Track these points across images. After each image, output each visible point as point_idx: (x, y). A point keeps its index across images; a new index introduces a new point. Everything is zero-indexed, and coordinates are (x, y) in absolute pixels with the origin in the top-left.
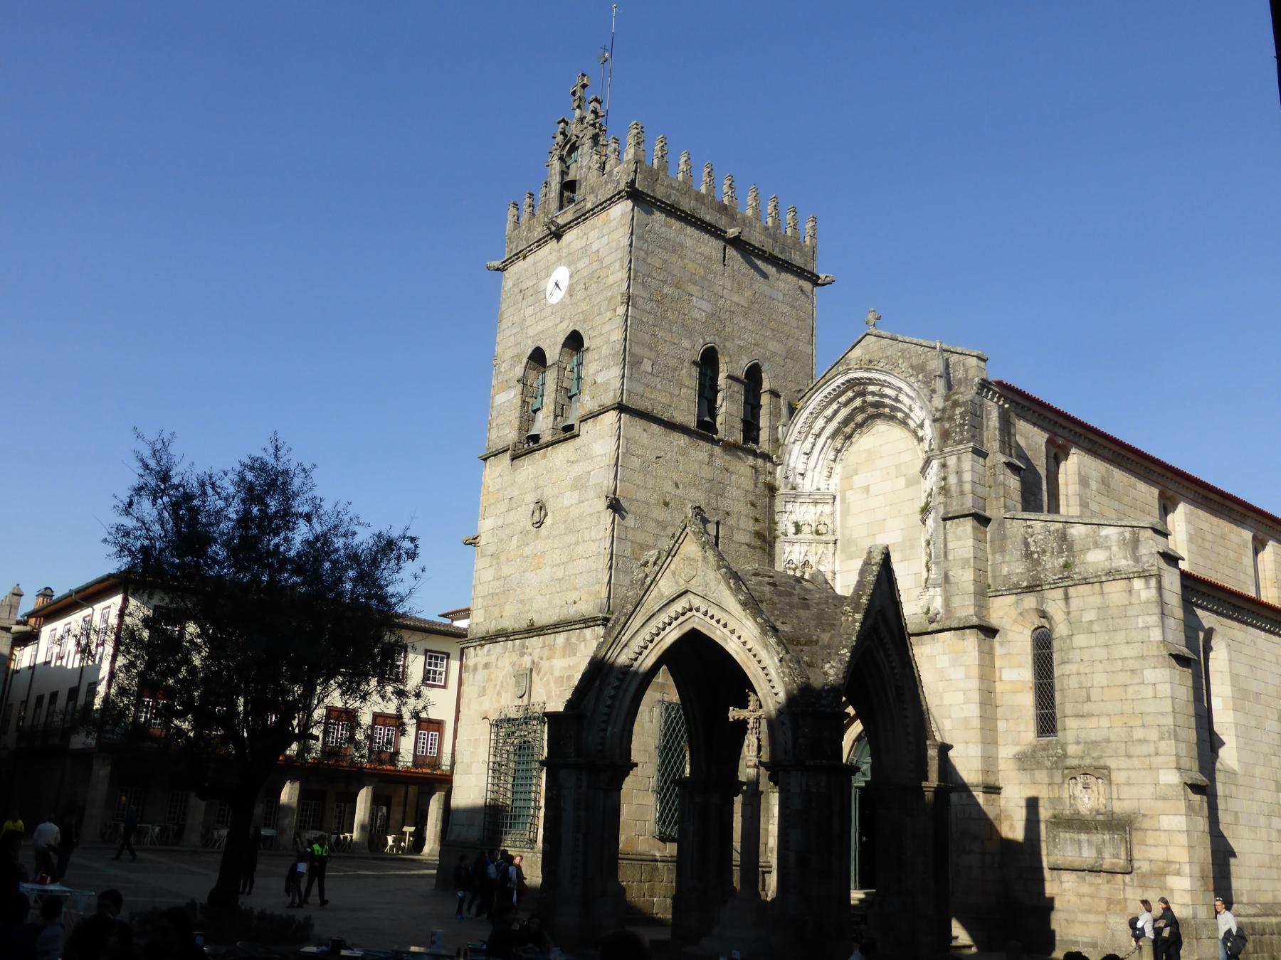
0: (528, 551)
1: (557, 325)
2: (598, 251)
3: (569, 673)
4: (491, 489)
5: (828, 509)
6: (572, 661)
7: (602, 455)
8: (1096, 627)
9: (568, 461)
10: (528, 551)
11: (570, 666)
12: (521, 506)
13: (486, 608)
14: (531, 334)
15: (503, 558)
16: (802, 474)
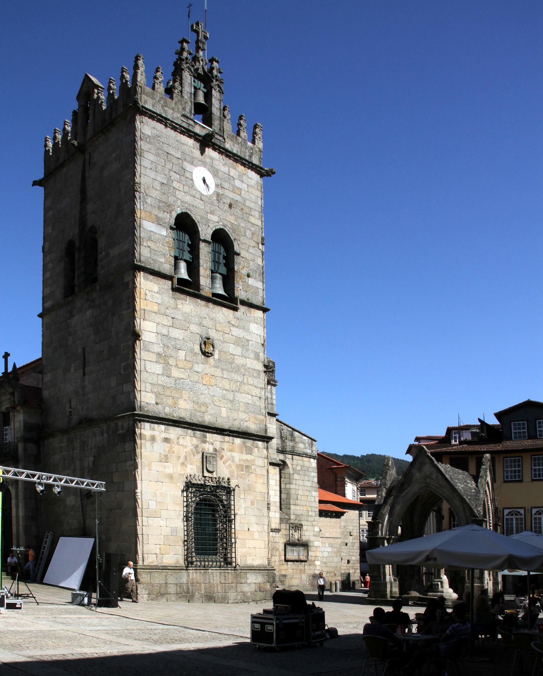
6: (249, 457)
8: (301, 472)
9: (229, 322)
12: (187, 330)
15: (172, 362)
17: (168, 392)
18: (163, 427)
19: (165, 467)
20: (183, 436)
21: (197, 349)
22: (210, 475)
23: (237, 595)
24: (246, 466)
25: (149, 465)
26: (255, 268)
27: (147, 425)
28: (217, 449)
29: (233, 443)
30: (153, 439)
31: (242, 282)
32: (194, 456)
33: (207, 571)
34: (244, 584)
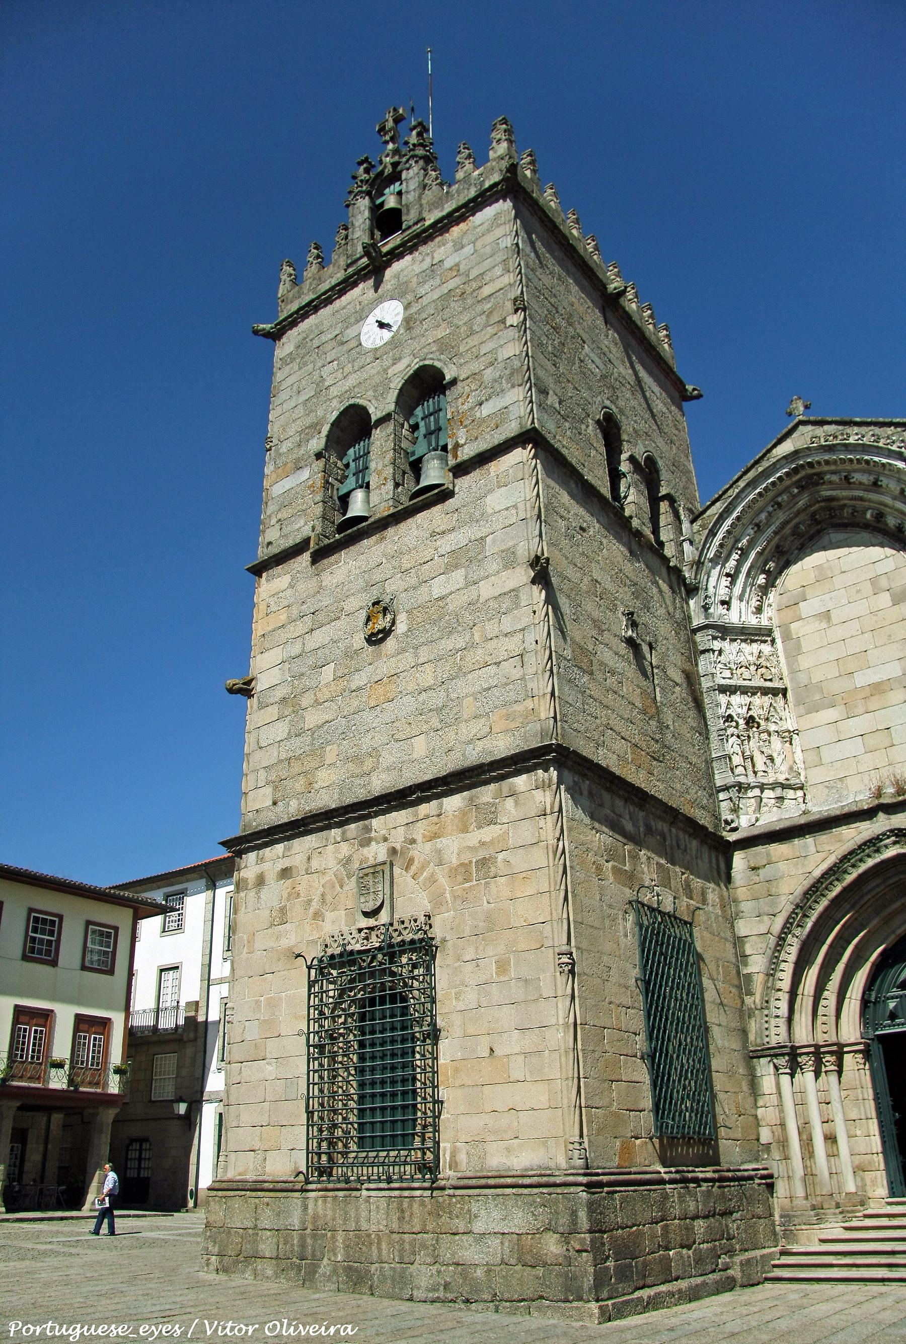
0: (358, 680)
1: (385, 371)
2: (457, 265)
3: (481, 854)
4: (273, 608)
5: (766, 648)
6: (488, 833)
7: (507, 509)
10: (358, 680)
11: (482, 844)
13: (276, 784)
14: (335, 394)
16: (723, 603)
17: (297, 767)
18: (279, 848)
19: (278, 938)
20: (320, 850)
21: (359, 640)
22: (371, 922)
23: (439, 1272)
24: (477, 862)
25: (251, 941)
26: (498, 374)
27: (252, 856)
28: (398, 847)
29: (439, 815)
30: (261, 881)
31: (466, 427)
32: (341, 887)
33: (355, 1193)
34: (465, 1237)
